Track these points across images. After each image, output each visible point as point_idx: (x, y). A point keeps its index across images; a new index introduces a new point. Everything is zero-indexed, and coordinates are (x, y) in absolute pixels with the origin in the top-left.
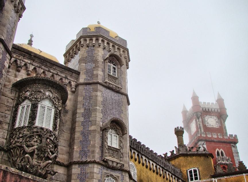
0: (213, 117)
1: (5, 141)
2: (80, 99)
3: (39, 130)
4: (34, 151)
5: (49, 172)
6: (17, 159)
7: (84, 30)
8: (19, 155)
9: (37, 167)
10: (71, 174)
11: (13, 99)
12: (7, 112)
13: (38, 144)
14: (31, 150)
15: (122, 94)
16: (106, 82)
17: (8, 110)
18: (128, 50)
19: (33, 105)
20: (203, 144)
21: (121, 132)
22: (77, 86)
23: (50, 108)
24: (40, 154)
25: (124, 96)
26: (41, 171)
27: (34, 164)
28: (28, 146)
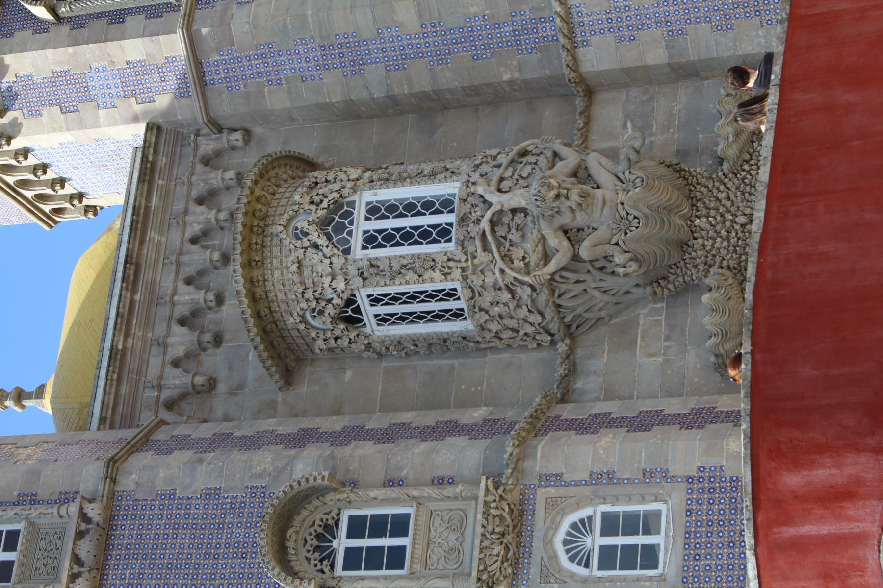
2: (277, 100)
5: (633, 156)
10: (623, 70)
19: (364, 279)
28: (546, 258)
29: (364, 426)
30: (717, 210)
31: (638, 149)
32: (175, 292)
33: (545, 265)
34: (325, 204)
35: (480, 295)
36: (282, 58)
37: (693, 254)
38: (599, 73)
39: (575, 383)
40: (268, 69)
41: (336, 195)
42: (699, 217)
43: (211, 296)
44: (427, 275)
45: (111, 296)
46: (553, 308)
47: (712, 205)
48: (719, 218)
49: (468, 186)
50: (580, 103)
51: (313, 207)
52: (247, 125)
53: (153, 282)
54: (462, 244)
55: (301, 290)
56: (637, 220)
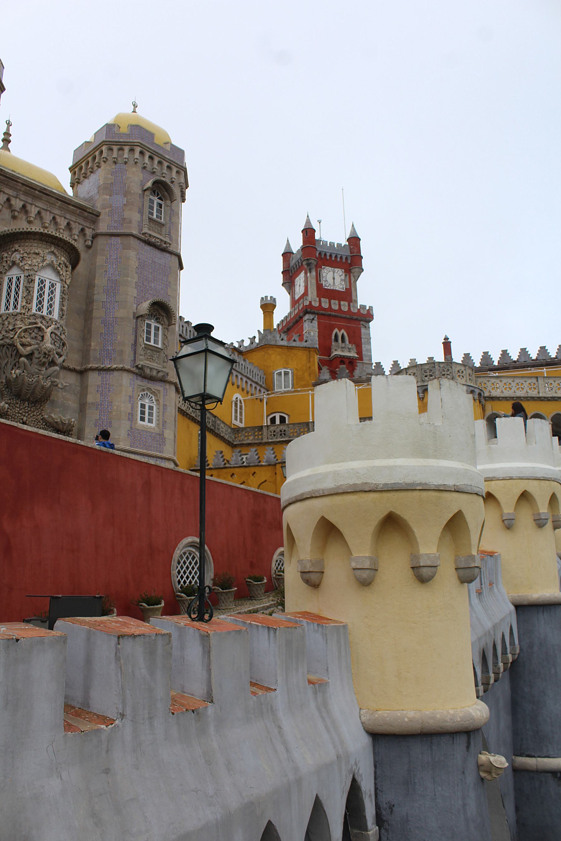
0: (336, 270)
2: (100, 260)
3: (38, 321)
5: (55, 384)
7: (109, 127)
15: (171, 253)
16: (143, 234)
18: (186, 169)
20: (313, 319)
21: (165, 320)
22: (95, 237)
23: (53, 282)
25: (173, 257)
28: (23, 345)
30: (30, 411)
32: (36, 206)
33: (20, 344)
34: (59, 268)
38: (88, 377)
41: (62, 273)
42: (28, 404)
43: (32, 219)
44: (25, 301)
45: (39, 183)
47: (32, 409)
50: (78, 368)
51: (58, 264)
52: (93, 247)
53: (41, 199)
54: (34, 315)
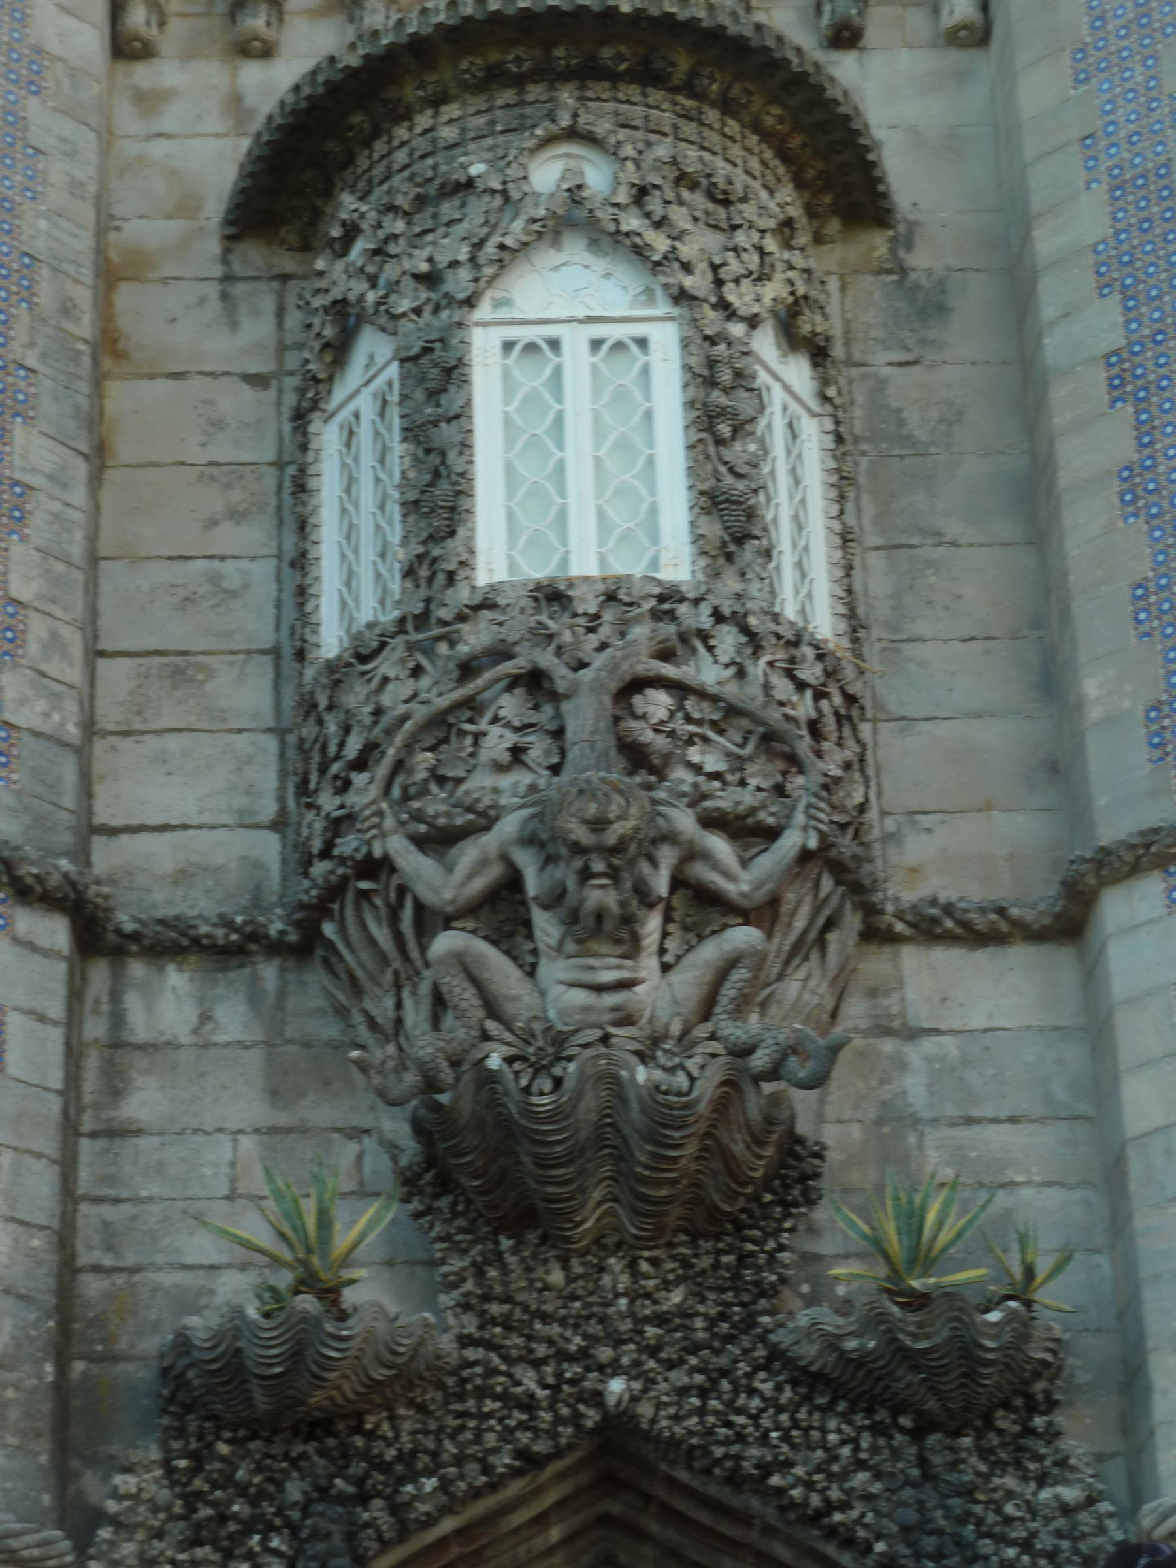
1: (269, 848)
4: (513, 882)
5: (760, 1060)
6: (399, 1005)
8: (397, 964)
9: (605, 1039)
11: (256, 380)
12: (229, 537)
13: (533, 788)
14: (470, 877)
17: (236, 515)
19: (415, 359)
24: (571, 884)
26: (671, 1070)
27: (562, 1013)
28: (438, 841)
29: (27, 419)
31: (783, 1072)
34: (632, 222)
35: (363, 673)
36: (1139, 69)
37: (511, 1260)
39: (181, 970)
40: (1113, 39)
41: (660, 243)
42: (632, 1266)
46: (333, 879)
48: (626, 1326)
49: (661, 598)
51: (622, 197)
55: (400, 201)
56: (547, 1086)
